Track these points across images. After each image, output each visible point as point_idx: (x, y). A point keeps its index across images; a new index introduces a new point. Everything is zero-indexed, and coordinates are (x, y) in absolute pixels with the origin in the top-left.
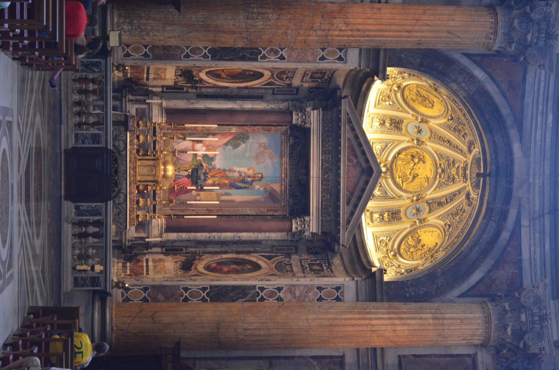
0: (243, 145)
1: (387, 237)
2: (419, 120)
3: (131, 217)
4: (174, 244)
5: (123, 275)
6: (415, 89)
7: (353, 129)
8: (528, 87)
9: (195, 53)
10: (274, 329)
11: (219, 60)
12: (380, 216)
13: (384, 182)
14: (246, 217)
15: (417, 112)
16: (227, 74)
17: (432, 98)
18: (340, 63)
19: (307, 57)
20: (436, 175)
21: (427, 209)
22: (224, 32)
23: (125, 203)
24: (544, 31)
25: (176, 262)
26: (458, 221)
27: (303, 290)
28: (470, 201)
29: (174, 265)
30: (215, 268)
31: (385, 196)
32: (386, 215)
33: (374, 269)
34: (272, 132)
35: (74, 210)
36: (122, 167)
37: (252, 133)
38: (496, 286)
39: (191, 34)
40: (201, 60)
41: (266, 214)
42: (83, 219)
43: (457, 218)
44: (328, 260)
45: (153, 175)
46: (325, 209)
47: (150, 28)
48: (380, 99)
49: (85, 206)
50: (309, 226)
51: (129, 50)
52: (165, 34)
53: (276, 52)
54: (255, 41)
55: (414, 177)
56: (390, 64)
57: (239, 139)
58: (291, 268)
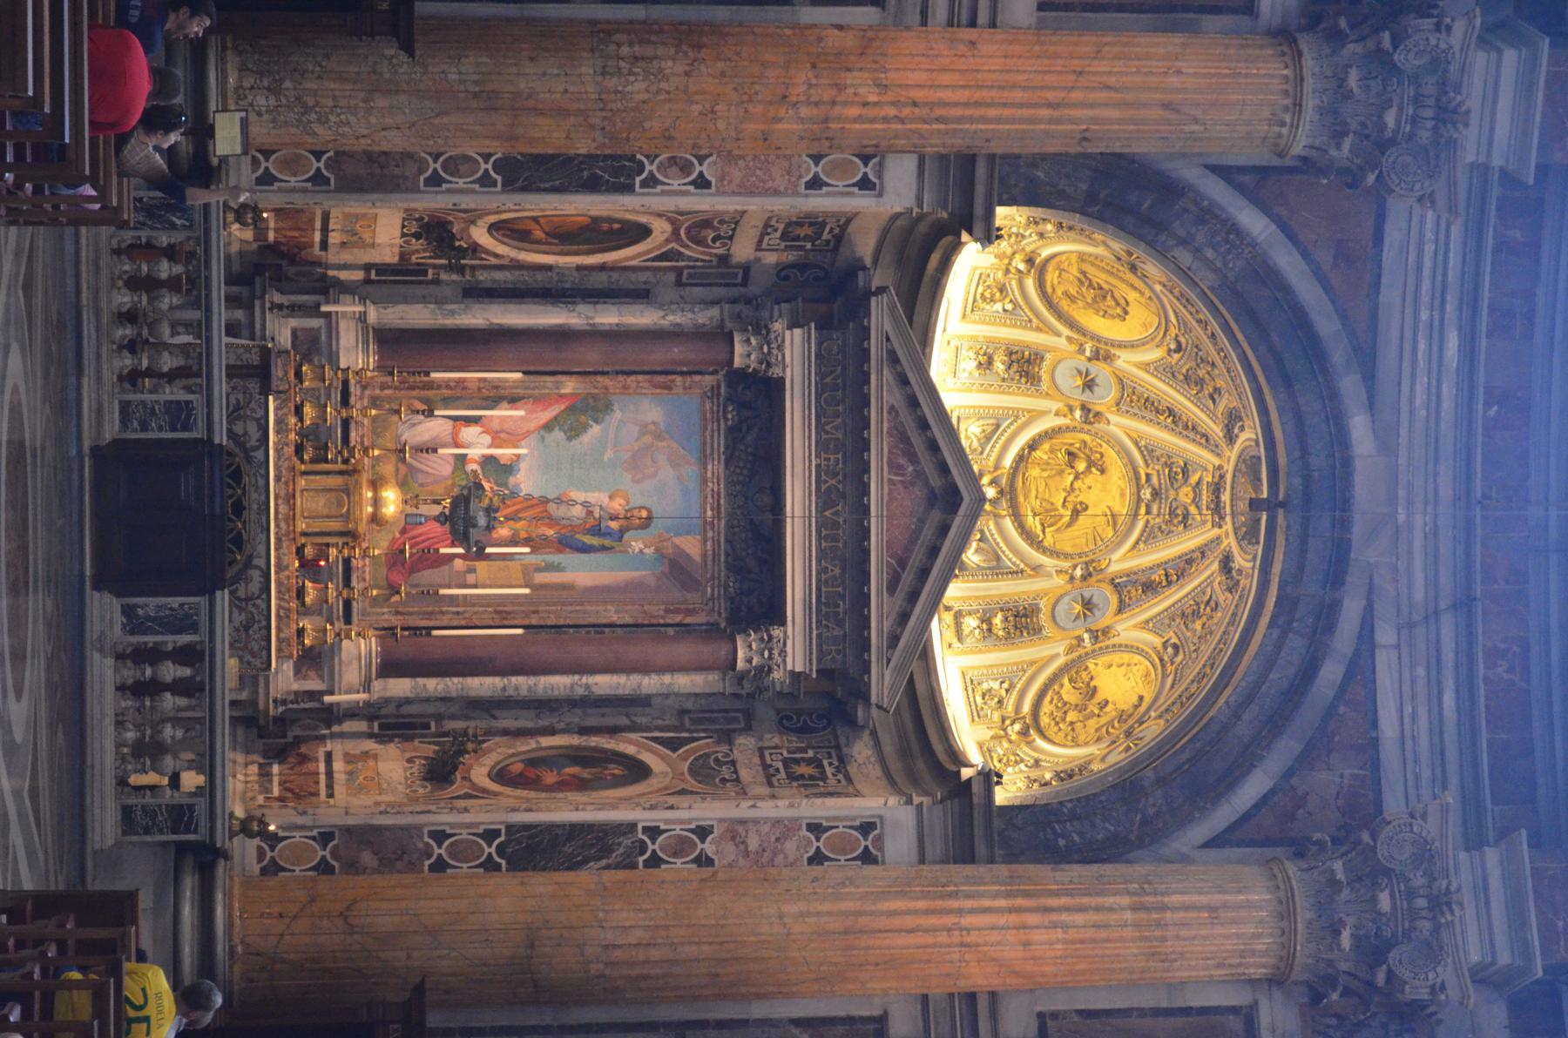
0: (595, 430)
1: (1002, 683)
2: (1088, 354)
3: (282, 635)
4: (406, 710)
5: (260, 799)
6: (1075, 266)
7: (903, 381)
8: (1389, 256)
9: (455, 173)
10: (690, 943)
11: (525, 189)
12: (982, 622)
13: (992, 527)
14: (607, 630)
15: (1082, 331)
16: (547, 229)
17: (1123, 290)
18: (862, 196)
19: (773, 180)
20: (1138, 507)
21: (1114, 600)
23: (264, 596)
24: (1432, 102)
25: (410, 761)
26: (1198, 633)
28: (1232, 578)
29: (405, 770)
30: (521, 775)
31: (996, 568)
33: (966, 773)
34: (674, 391)
35: (119, 618)
36: (254, 496)
37: (621, 394)
38: (1309, 813)
39: (446, 120)
40: (473, 191)
41: (662, 621)
42: (146, 643)
43: (1198, 625)
44: (838, 747)
45: (342, 516)
46: (827, 605)
47: (330, 103)
48: (978, 296)
49: (150, 605)
50: (783, 652)
51: (269, 165)
52: (373, 120)
53: (686, 168)
54: (624, 135)
55: (1076, 513)
56: (1005, 197)
57: (584, 411)
58: (736, 772)
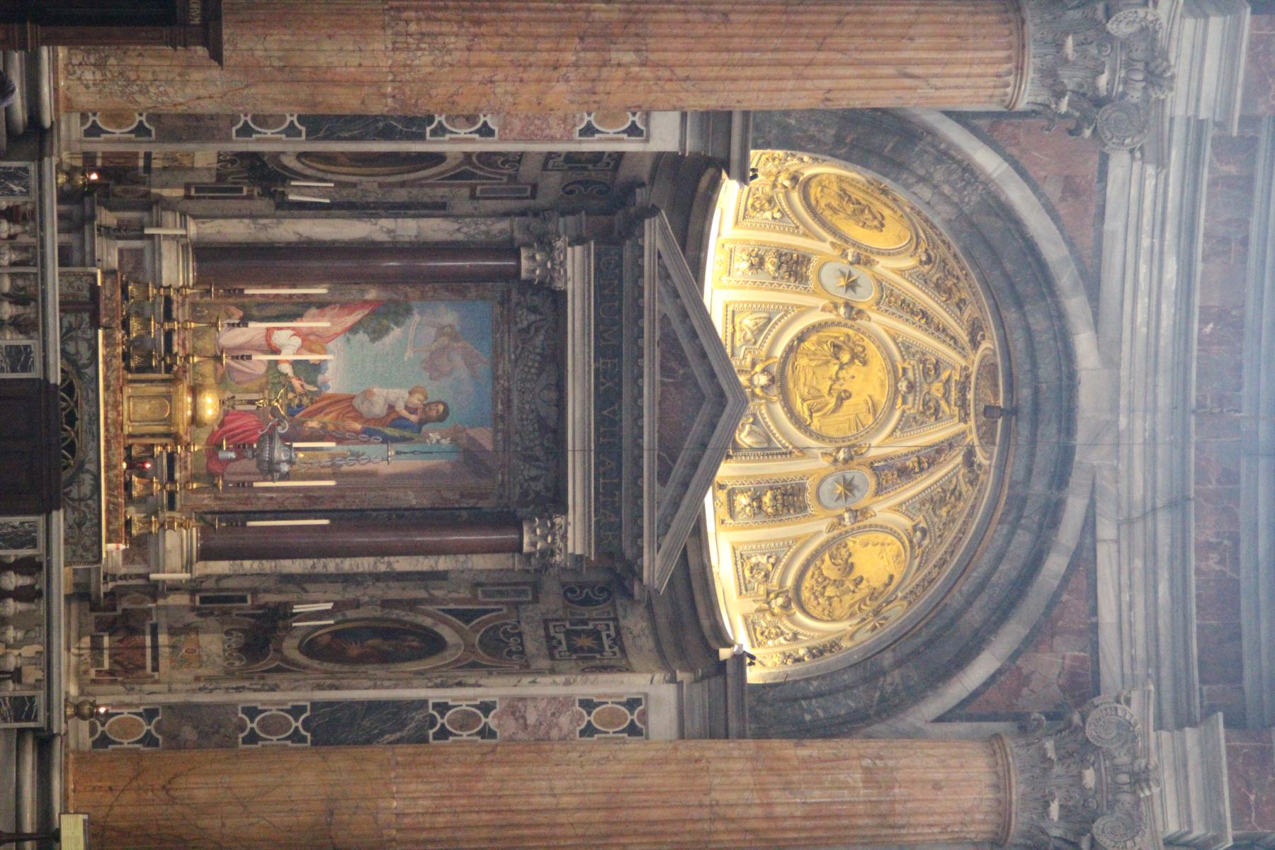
0: (396, 332)
2: (850, 258)
5: (93, 672)
8: (1112, 190)
10: (470, 812)
12: (753, 500)
13: (764, 411)
15: (846, 239)
21: (872, 482)
22: (335, 83)
23: (95, 497)
24: (1140, 66)
25: (227, 633)
26: (944, 519)
27: (544, 710)
29: (224, 643)
31: (768, 450)
32: (767, 499)
33: (725, 653)
36: (85, 407)
43: (943, 512)
44: (616, 619)
46: (604, 495)
47: (150, 77)
50: (564, 537)
53: (471, 119)
57: (386, 315)
58: (522, 644)
